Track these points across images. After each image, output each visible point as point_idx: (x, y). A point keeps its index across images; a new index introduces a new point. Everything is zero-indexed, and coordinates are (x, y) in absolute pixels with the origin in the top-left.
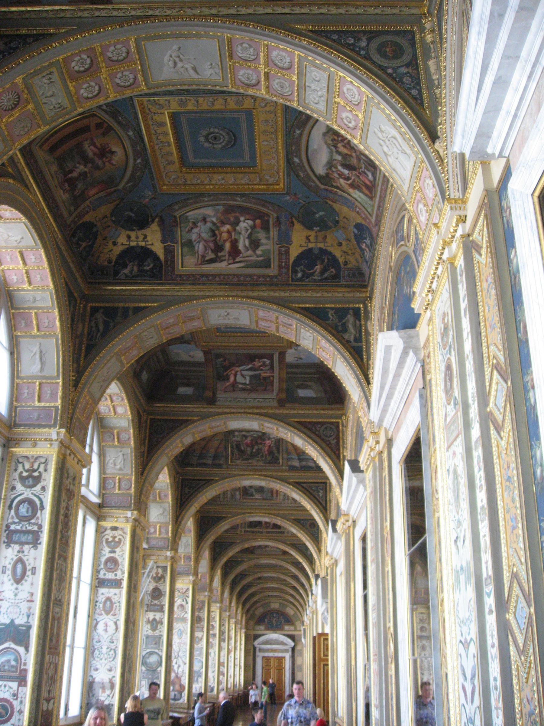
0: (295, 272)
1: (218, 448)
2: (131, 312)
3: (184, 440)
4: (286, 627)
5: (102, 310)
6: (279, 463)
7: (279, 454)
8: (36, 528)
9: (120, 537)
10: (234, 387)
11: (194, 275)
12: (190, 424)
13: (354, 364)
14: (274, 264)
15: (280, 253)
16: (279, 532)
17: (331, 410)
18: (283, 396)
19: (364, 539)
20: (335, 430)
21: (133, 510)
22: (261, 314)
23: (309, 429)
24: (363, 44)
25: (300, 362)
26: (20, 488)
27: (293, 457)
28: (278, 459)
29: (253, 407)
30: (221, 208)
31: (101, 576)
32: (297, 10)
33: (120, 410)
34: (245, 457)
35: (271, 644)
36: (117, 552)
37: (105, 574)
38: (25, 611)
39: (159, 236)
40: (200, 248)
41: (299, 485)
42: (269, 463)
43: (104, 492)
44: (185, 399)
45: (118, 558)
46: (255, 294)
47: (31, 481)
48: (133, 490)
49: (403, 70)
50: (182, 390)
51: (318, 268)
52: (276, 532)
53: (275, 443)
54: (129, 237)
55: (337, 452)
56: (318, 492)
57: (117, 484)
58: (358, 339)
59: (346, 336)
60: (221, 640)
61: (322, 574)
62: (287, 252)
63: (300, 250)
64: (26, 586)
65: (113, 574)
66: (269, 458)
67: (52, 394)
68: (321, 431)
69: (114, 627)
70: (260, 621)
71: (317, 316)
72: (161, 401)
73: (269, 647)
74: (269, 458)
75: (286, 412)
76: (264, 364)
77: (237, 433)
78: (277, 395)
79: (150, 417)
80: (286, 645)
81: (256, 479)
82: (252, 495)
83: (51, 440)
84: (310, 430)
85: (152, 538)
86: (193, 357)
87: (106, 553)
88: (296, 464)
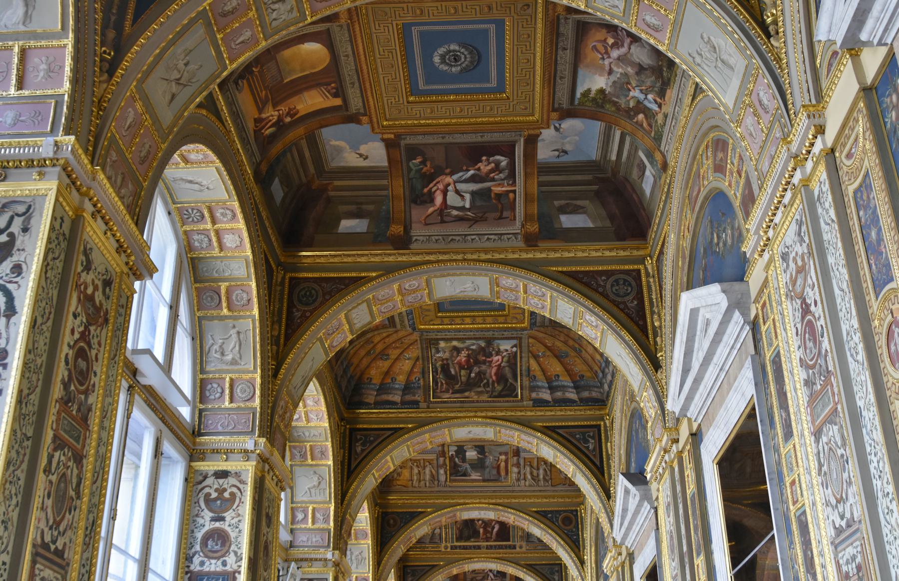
1: (411, 372)
3: (353, 314)
6: (516, 396)
7: (517, 381)
9: (234, 490)
12: (364, 285)
16: (506, 547)
17: (624, 249)
18: (534, 228)
20: (633, 283)
21: (259, 436)
23: (584, 284)
25: (565, 159)
27: (540, 384)
28: (515, 389)
29: (478, 251)
31: (195, 566)
33: (230, 241)
34: (457, 387)
36: (228, 519)
37: (202, 564)
43: (202, 406)
44: (352, 241)
45: (228, 529)
48: (257, 402)
50: (347, 225)
52: (500, 547)
53: (508, 361)
55: (641, 323)
56: (587, 442)
57: (227, 392)
65: (219, 563)
66: (499, 388)
67: (50, 70)
68: (608, 286)
72: (309, 246)
74: (499, 388)
75: (539, 255)
76: (497, 168)
77: (442, 344)
78: (523, 226)
79: (288, 275)
81: (478, 424)
82: (465, 475)
84: (587, 285)
85: (301, 529)
86: (366, 158)
87: (206, 522)
88: (546, 395)
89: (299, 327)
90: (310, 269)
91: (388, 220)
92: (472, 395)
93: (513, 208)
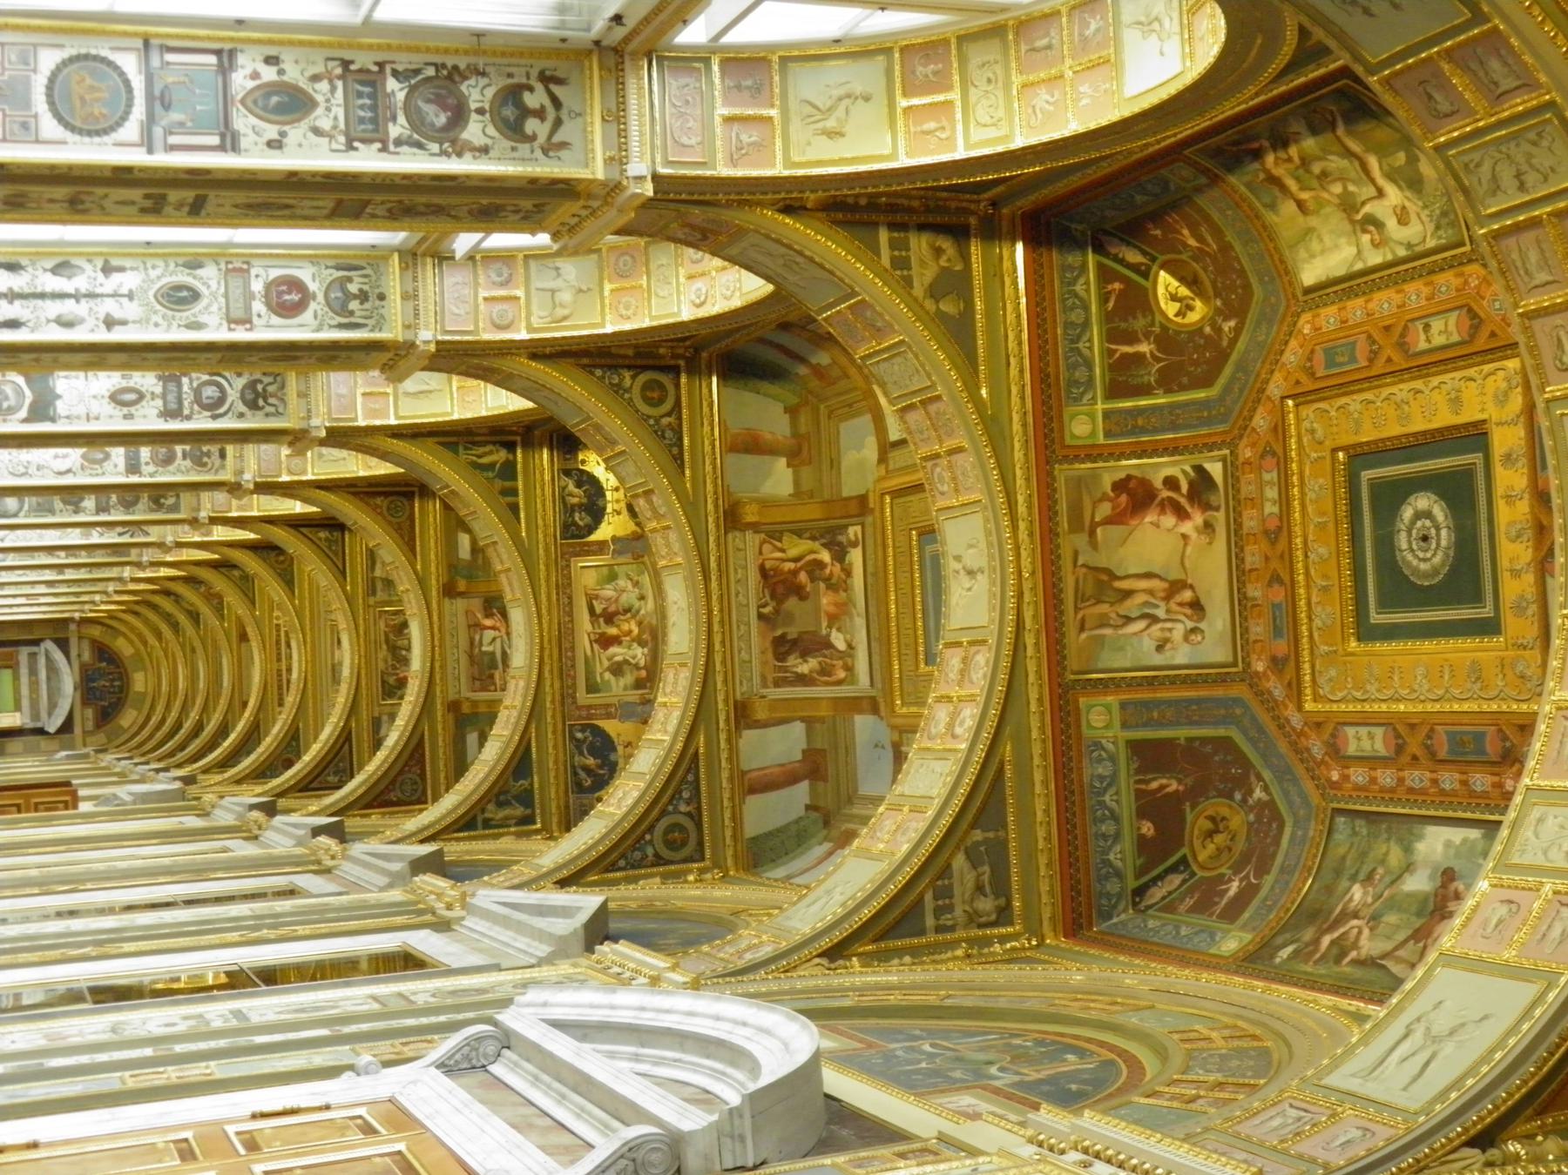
0: (583, 728)
2: (510, 499)
4: (89, 713)
5: (511, 457)
8: (186, 412)
10: (476, 626)
11: (570, 585)
13: (449, 820)
14: (594, 699)
15: (608, 705)
18: (466, 709)
19: (225, 850)
22: (522, 683)
24: (683, 808)
26: (240, 383)
30: (654, 622)
32: (723, 736)
34: (392, 636)
35: (48, 678)
38: (74, 412)
39: (621, 533)
40: (608, 592)
41: (345, 738)
42: (383, 682)
46: (547, 674)
47: (250, 396)
49: (650, 851)
51: (591, 761)
54: (617, 489)
56: (335, 773)
58: (487, 824)
59: (491, 807)
60: (49, 583)
61: (193, 790)
62: (609, 716)
63: (613, 734)
64: (108, 408)
66: (392, 680)
69: (63, 469)
70: (103, 652)
71: (520, 764)
73: (43, 674)
74: (392, 680)
75: (439, 714)
80: (50, 715)
81: (352, 659)
83: (309, 417)
84: (411, 756)
88: (383, 732)
89: (367, 504)
90: (421, 509)
91: (469, 578)
92: (383, 652)
93: (484, 689)
